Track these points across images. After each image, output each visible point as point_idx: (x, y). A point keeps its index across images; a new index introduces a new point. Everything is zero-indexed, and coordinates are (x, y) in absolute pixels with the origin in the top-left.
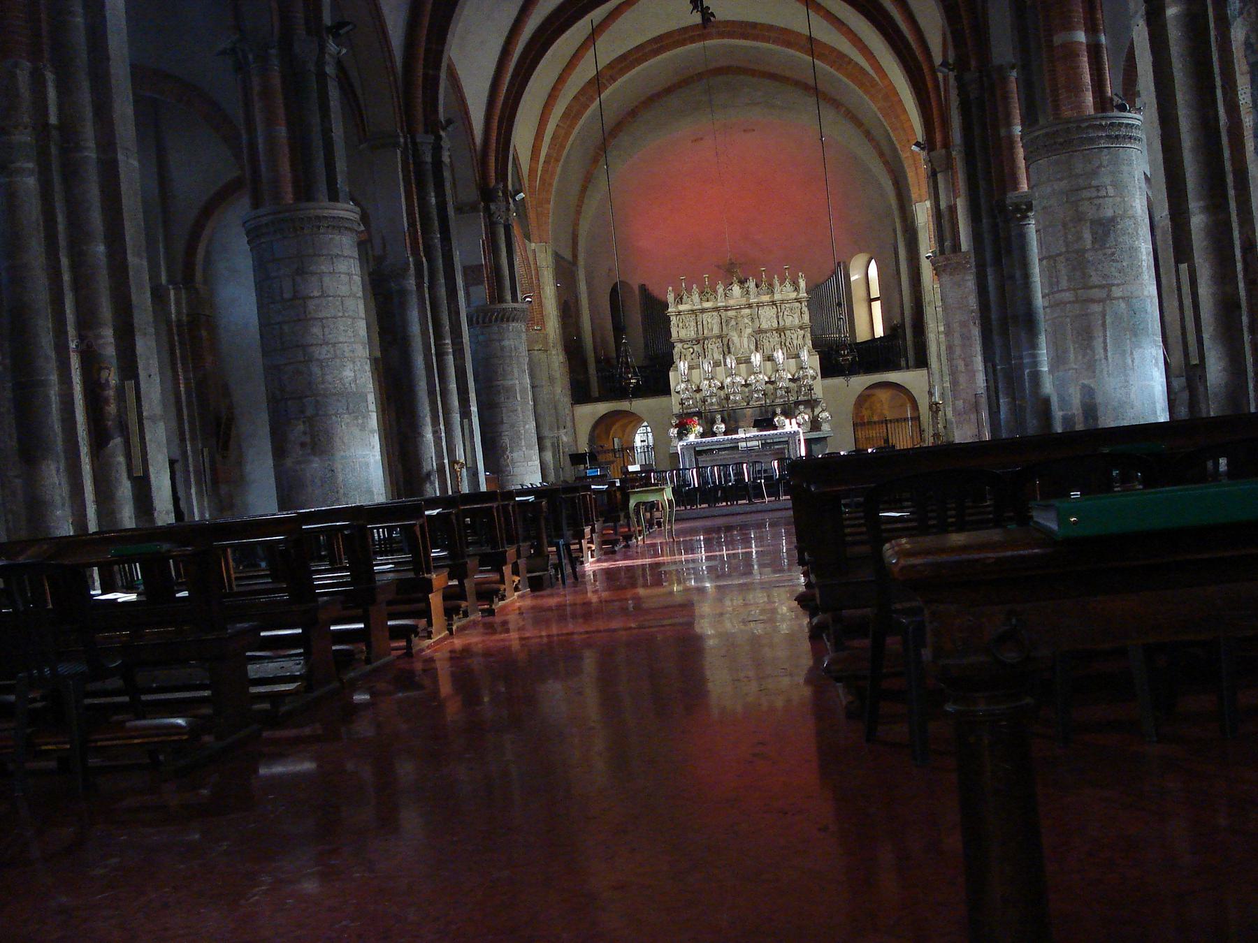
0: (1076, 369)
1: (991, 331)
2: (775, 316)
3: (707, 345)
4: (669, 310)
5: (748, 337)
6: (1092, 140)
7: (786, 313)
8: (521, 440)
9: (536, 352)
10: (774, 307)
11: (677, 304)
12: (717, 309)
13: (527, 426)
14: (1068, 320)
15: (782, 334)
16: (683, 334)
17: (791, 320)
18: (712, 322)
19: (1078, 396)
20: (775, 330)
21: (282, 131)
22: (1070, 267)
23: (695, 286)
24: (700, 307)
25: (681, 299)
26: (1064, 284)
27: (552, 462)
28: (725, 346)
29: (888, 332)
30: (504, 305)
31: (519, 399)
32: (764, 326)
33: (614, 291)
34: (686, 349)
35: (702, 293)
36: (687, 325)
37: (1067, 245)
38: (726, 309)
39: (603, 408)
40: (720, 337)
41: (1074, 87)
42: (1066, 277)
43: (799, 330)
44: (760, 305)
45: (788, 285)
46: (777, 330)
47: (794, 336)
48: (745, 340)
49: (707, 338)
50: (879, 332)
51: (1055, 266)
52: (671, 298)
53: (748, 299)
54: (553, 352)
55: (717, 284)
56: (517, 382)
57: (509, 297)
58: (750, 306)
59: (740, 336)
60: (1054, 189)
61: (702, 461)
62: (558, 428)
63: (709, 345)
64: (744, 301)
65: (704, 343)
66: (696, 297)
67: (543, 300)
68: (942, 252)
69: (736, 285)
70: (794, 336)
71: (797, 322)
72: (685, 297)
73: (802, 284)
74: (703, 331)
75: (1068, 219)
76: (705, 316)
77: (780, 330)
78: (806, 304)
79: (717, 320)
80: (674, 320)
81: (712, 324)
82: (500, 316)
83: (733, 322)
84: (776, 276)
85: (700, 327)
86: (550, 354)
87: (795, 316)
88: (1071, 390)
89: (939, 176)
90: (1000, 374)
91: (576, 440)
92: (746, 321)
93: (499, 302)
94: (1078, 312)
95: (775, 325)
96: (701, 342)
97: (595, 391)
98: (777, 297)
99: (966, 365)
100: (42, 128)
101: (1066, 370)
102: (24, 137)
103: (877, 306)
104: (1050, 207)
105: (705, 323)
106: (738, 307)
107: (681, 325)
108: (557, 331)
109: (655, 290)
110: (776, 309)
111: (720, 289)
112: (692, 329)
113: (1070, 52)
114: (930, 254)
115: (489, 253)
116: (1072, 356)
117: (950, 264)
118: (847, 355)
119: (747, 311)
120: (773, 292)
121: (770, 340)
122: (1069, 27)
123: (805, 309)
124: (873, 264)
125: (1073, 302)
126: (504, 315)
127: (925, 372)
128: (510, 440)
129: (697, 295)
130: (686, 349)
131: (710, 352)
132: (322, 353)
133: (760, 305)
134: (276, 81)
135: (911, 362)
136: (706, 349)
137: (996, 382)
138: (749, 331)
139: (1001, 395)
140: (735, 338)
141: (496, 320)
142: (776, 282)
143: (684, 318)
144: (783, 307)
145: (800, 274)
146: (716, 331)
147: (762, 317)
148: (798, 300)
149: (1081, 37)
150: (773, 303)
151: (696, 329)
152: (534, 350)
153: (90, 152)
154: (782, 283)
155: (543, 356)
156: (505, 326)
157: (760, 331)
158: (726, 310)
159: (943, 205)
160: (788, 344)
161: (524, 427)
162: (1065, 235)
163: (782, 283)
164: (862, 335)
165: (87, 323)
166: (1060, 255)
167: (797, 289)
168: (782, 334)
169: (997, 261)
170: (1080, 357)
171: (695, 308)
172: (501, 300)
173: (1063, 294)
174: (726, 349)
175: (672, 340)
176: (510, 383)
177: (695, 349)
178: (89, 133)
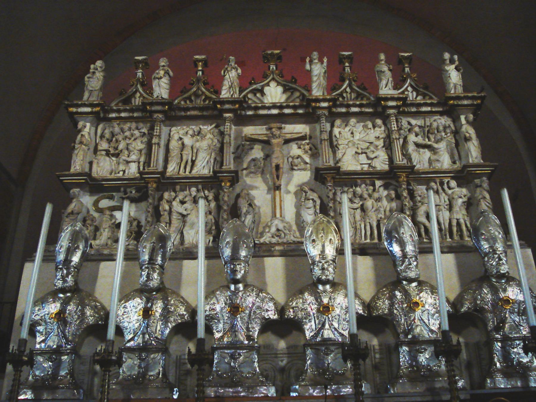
2: (381, 143)
3: (170, 202)
7: (412, 138)
10: (379, 122)
23: (163, 62)
34: (100, 211)
43: (453, 183)
63: (174, 203)
69: (273, 84)
81: (195, 151)
83: (257, 153)
84: (382, 57)
92: (299, 152)
105: (174, 144)
106: (275, 112)
112: (133, 157)
121: (369, 203)
123: (469, 130)
130: (100, 211)
131: (176, 223)
145: (447, 56)
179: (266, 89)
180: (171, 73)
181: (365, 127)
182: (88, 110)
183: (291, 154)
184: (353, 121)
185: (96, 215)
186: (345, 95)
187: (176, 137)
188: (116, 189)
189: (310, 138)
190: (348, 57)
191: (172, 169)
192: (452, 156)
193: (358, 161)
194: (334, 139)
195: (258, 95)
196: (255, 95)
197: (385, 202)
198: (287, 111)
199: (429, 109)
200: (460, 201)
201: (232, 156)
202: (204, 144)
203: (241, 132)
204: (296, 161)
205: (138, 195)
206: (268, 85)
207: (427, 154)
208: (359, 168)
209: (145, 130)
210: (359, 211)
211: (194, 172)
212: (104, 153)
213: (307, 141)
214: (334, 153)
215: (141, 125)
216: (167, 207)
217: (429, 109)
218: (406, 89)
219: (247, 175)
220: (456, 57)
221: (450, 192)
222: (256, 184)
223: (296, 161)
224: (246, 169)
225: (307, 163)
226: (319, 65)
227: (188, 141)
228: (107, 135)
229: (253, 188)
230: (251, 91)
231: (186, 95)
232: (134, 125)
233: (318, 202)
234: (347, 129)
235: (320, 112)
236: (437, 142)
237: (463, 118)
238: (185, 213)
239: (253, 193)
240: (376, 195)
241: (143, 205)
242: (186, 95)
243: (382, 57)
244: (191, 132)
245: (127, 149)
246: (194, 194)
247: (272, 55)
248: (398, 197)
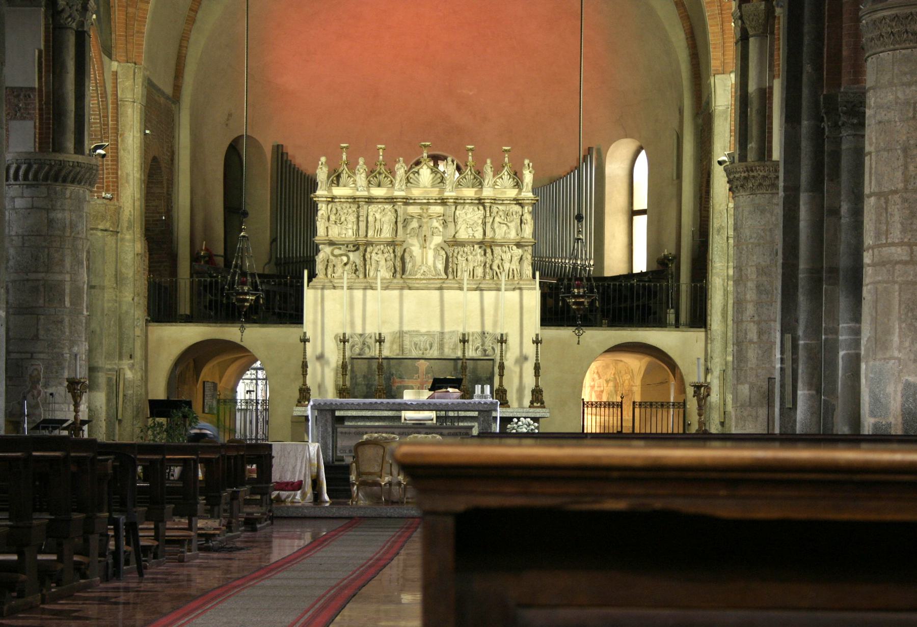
0: (899, 359)
1: (796, 287)
2: (480, 221)
3: (371, 253)
4: (318, 193)
5: (435, 250)
7: (497, 219)
8: (63, 369)
9: (100, 234)
10: (481, 208)
11: (331, 186)
12: (391, 200)
13: (75, 349)
14: (897, 287)
15: (489, 251)
16: (335, 233)
17: (506, 231)
19: (899, 398)
20: (478, 243)
22: (908, 212)
23: (361, 161)
24: (365, 194)
25: (338, 177)
26: (896, 234)
27: (104, 408)
28: (398, 259)
29: (655, 267)
30: (61, 157)
31: (67, 304)
32: (463, 235)
33: (233, 151)
34: (336, 256)
35: (372, 172)
36: (343, 219)
37: (906, 181)
38: (407, 201)
40: (392, 244)
42: (899, 226)
43: (515, 248)
44: (458, 202)
45: (506, 177)
46: (481, 244)
47: (506, 257)
48: (430, 254)
49: (371, 244)
50: (640, 265)
51: (886, 209)
52: (322, 174)
53: (442, 191)
54: (128, 237)
55: (396, 162)
56: (68, 277)
57: (70, 145)
58: (443, 202)
59: (423, 247)
60: (898, 97)
61: (342, 433)
62: (121, 357)
63: (373, 255)
64: (434, 193)
65: (365, 251)
66: (361, 178)
67: (121, 153)
68: (743, 157)
69: (425, 167)
70: (509, 255)
71: (513, 235)
72: (344, 176)
73: (528, 177)
74: (367, 232)
75: (912, 142)
76: (373, 208)
77: (486, 245)
78: (531, 208)
79: (389, 217)
80: (323, 209)
81: (382, 223)
82: (52, 172)
83: (414, 224)
84: (489, 161)
85: (362, 225)
86: (122, 240)
87: (512, 225)
88: (890, 389)
89: (751, 40)
90: (802, 353)
91: (145, 379)
92: (435, 224)
93: (54, 151)
94: (911, 277)
95: (479, 236)
96: (362, 248)
97: (184, 308)
98: (487, 192)
99: (760, 333)
101: (885, 359)
103: (641, 223)
104: (889, 121)
105: (371, 219)
107: (333, 218)
108: (137, 204)
109: (299, 159)
110: (483, 212)
111: (401, 170)
112: (350, 226)
114: (725, 159)
115: (47, 71)
116: (896, 339)
117: (754, 177)
118: (582, 297)
119: (439, 209)
120: (481, 184)
121: (470, 258)
123: (528, 217)
124: (643, 157)
125: (905, 263)
126: (60, 170)
127: (699, 334)
128: (46, 368)
129: (364, 175)
130: (336, 256)
133: (458, 202)
135: (683, 317)
136: (368, 262)
137: (795, 361)
138: (438, 240)
139: (800, 384)
140: (416, 250)
141: (46, 178)
142: (488, 170)
143: (339, 208)
144: (495, 209)
145: (526, 162)
146: (387, 234)
147: (460, 221)
148: (519, 202)
150: (480, 202)
151: (355, 227)
152: (97, 229)
154: (497, 171)
155: (110, 240)
156: (58, 188)
157: (455, 243)
158: (406, 204)
159: (752, 87)
160: (495, 267)
161: (70, 349)
162: (906, 167)
163: (497, 171)
164: (614, 266)
166: (895, 192)
167: (518, 185)
168: (489, 251)
169: (817, 185)
170: (907, 344)
171: (358, 194)
172: (58, 147)
173: (893, 249)
174: (398, 264)
175: (317, 239)
176: (59, 277)
177: (351, 258)
179: (421, 171)
180: (367, 170)
181: (473, 210)
182: (325, 199)
183: (433, 226)
184: (467, 206)
185: (333, 258)
186: (467, 177)
187: (371, 214)
188: (343, 245)
189: (444, 215)
190: (471, 150)
191: (370, 233)
192: (517, 231)
193: (467, 232)
194: (456, 217)
195: (416, 175)
196: (414, 174)
197: (479, 256)
198: (431, 201)
199: (509, 202)
200: (516, 258)
201: (402, 225)
202: (386, 219)
203: (406, 209)
204: (435, 230)
205: (355, 248)
206: (422, 168)
207: (505, 228)
208: (467, 237)
209: (354, 209)
210: (465, 261)
211: (382, 236)
212: (334, 222)
213: (441, 218)
214: (455, 226)
215: (352, 205)
216: (369, 256)
217: (509, 202)
218: (504, 174)
219: (409, 238)
220: (531, 164)
221: (512, 252)
222: (414, 243)
223: (435, 230)
224: (409, 234)
225: (440, 232)
226: (451, 167)
227: (378, 216)
228: (334, 211)
229: (412, 245)
230: (412, 173)
231: (374, 174)
232: (348, 205)
233: (445, 256)
234: (464, 211)
235: (448, 204)
236: (511, 222)
237: (526, 208)
238: (378, 260)
239: (413, 248)
240: (474, 253)
241: (357, 253)
242: (374, 174)
243: (489, 161)
244: (379, 211)
245: (346, 220)
246: (382, 249)
247: (425, 146)
248: (485, 254)
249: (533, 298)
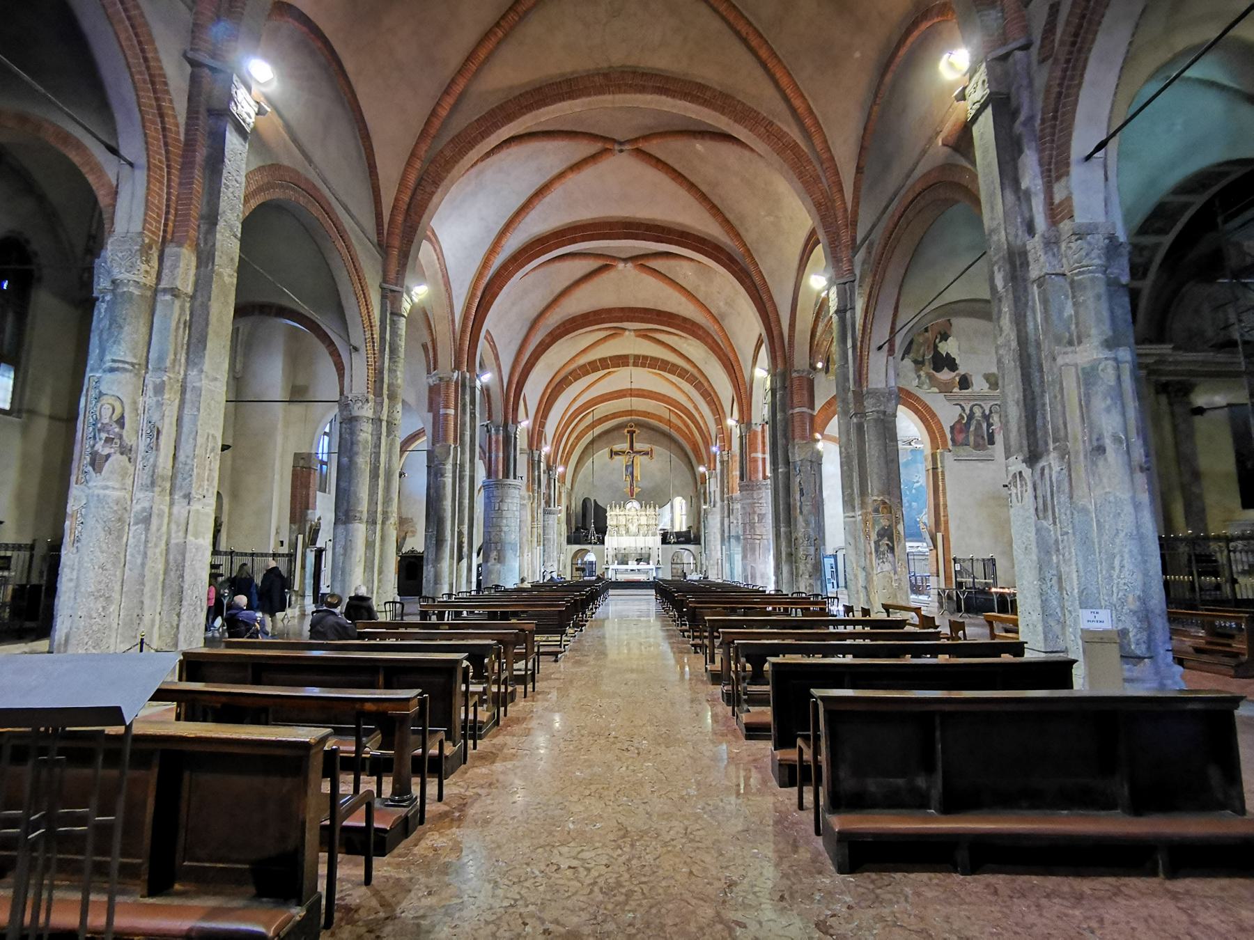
6: (760, 489)
18: (622, 520)
21: (501, 455)
33: (584, 501)
39: (577, 547)
41: (756, 471)
52: (608, 509)
100: (455, 465)
102: (449, 467)
113: (755, 460)
122: (756, 451)
132: (505, 529)
134: (501, 438)
149: (760, 455)
153: (467, 473)
164: (677, 529)
165: (461, 523)
178: (467, 466)
249: (659, 538)
